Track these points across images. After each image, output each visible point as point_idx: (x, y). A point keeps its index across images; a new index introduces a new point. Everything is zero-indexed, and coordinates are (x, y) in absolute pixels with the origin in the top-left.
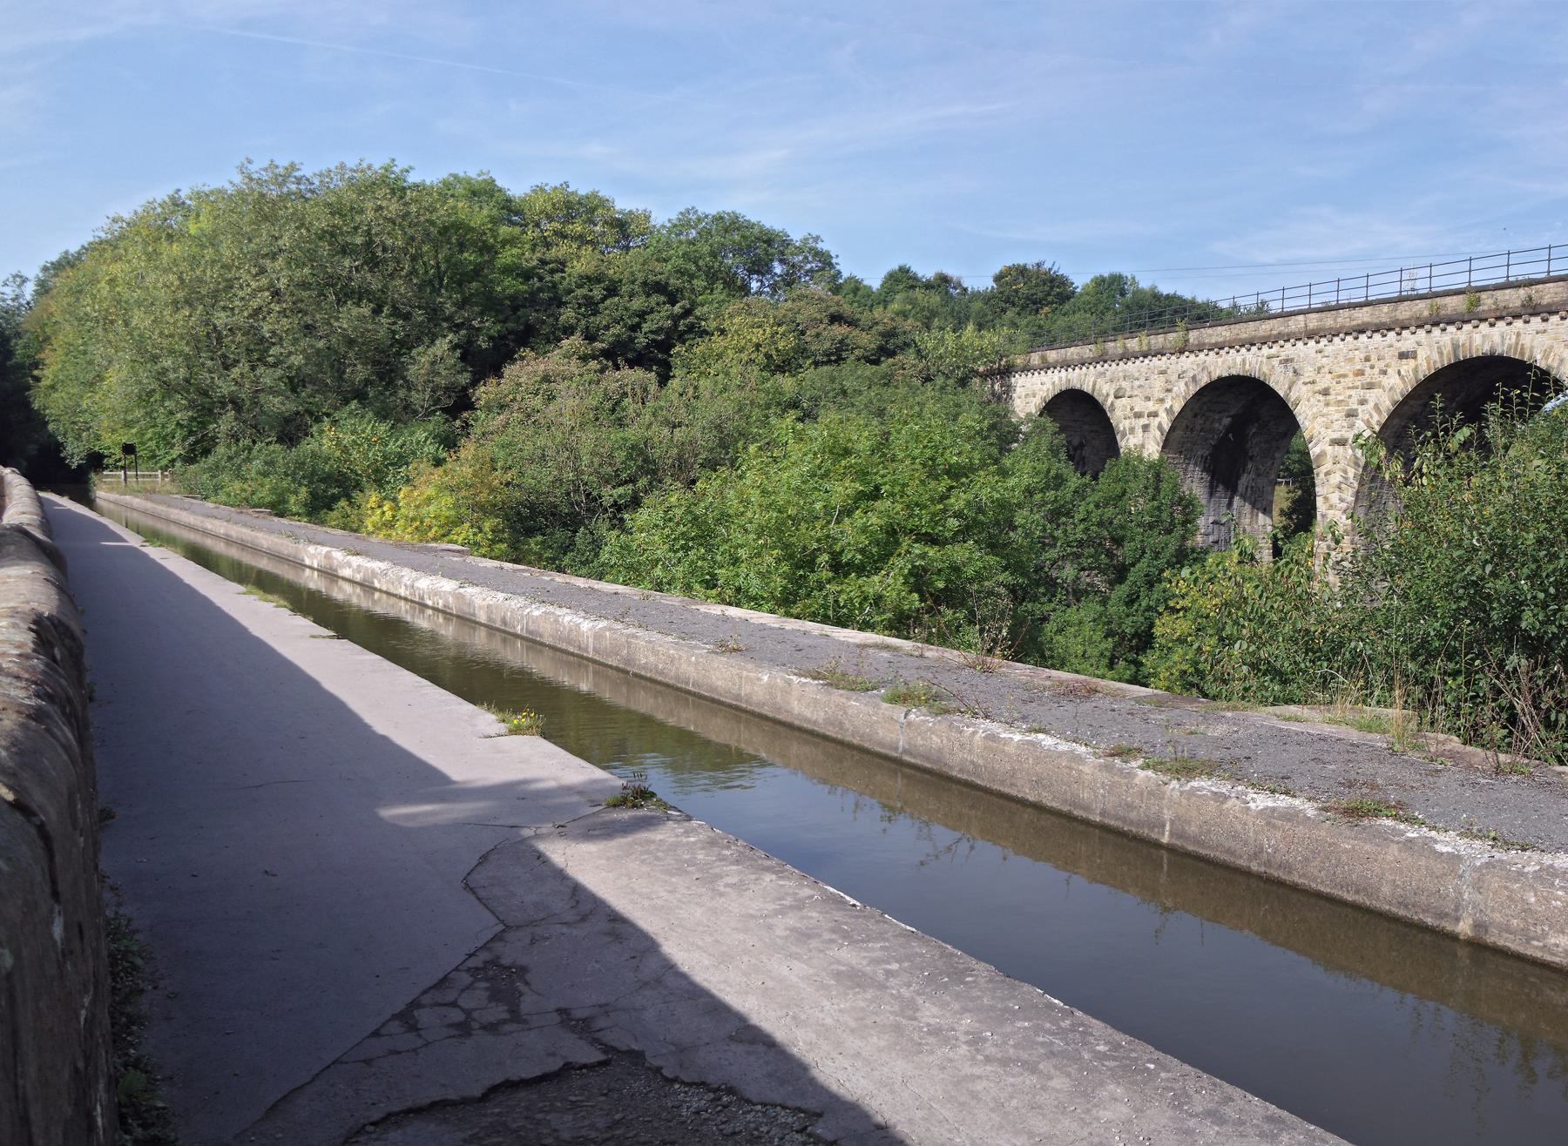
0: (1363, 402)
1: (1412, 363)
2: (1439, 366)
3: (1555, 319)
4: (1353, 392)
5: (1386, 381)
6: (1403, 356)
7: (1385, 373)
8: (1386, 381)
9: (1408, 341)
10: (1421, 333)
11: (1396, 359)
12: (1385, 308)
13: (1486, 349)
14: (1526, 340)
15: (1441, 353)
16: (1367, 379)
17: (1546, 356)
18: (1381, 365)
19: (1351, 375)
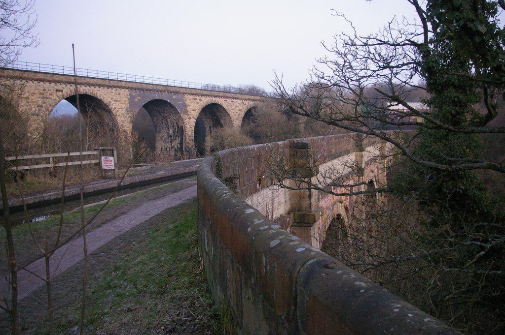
0: (44, 103)
1: (61, 93)
2: (71, 95)
3: (102, 88)
4: (40, 99)
5: (52, 97)
6: (57, 90)
7: (52, 95)
8: (52, 97)
9: (59, 86)
10: (63, 85)
11: (55, 92)
12: (49, 75)
13: (85, 92)
14: (95, 92)
15: (71, 91)
16: (45, 95)
17: (100, 96)
18: (50, 92)
19: (38, 94)
